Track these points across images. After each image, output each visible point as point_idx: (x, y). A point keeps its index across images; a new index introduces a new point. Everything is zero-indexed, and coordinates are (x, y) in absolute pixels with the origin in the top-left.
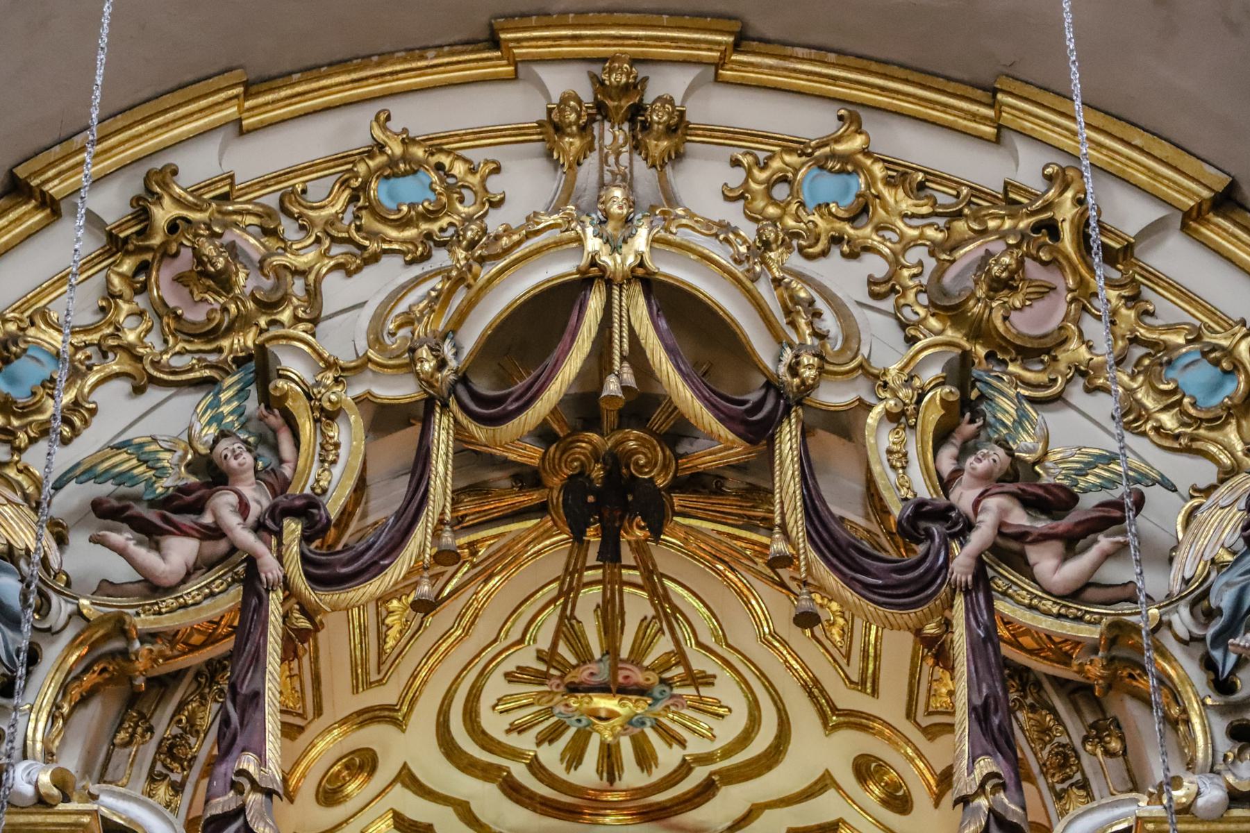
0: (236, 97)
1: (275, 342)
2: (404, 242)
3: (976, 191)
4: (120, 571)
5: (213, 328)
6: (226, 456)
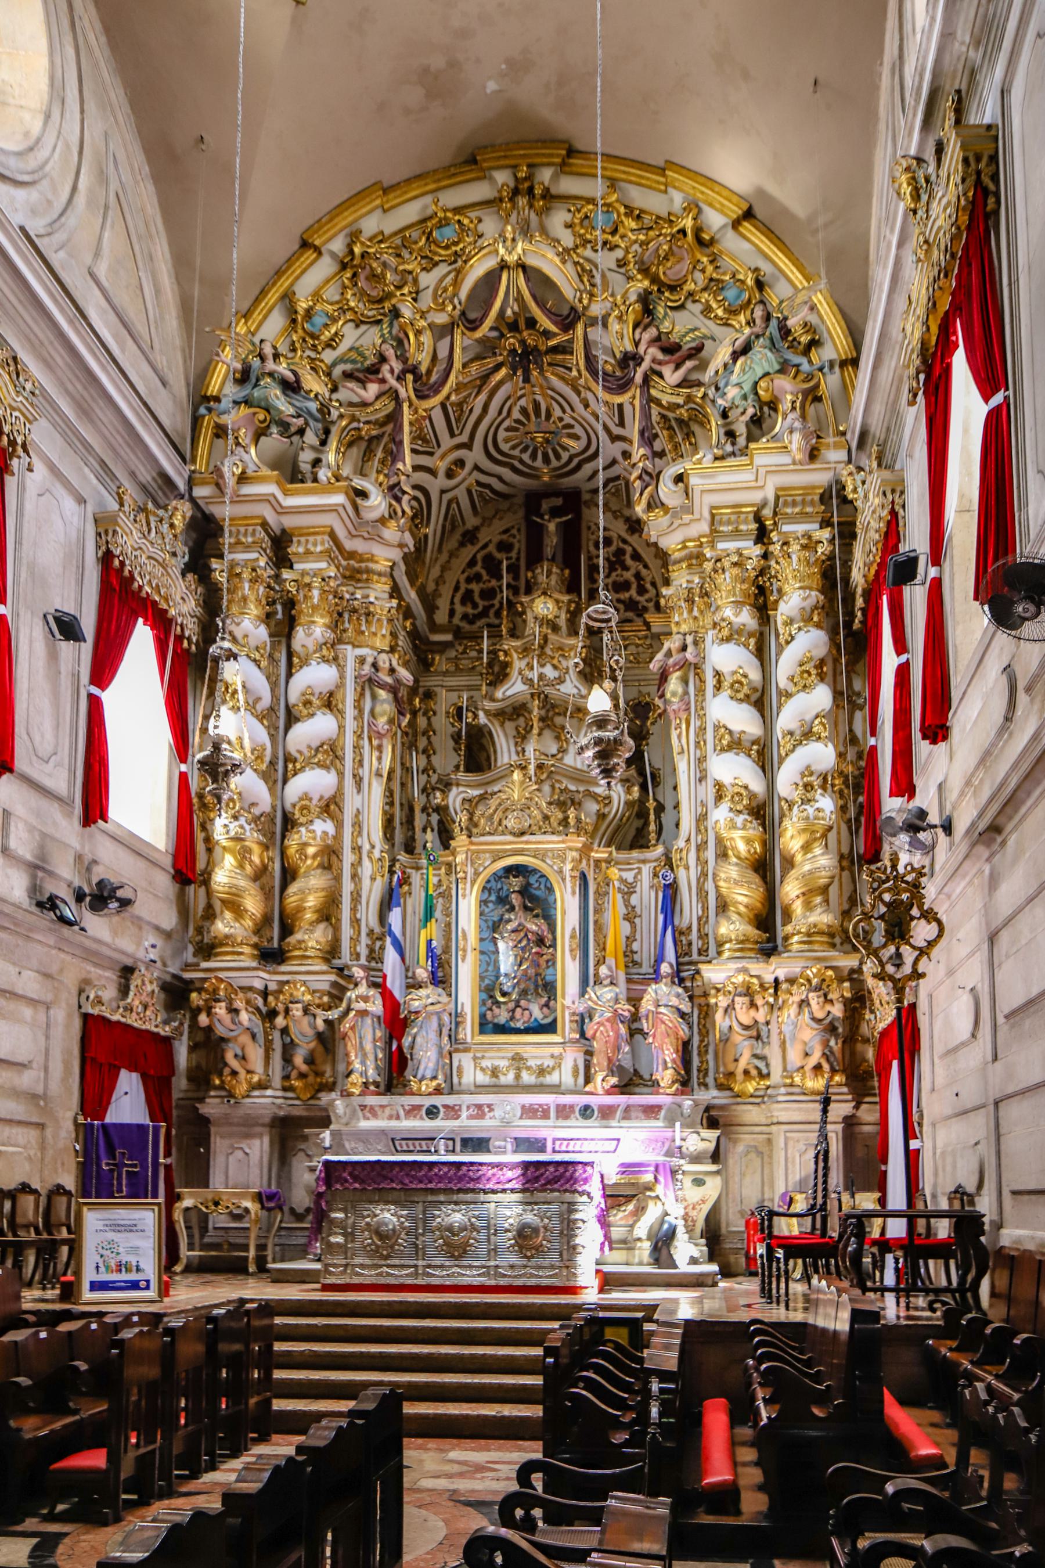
3: (658, 217)
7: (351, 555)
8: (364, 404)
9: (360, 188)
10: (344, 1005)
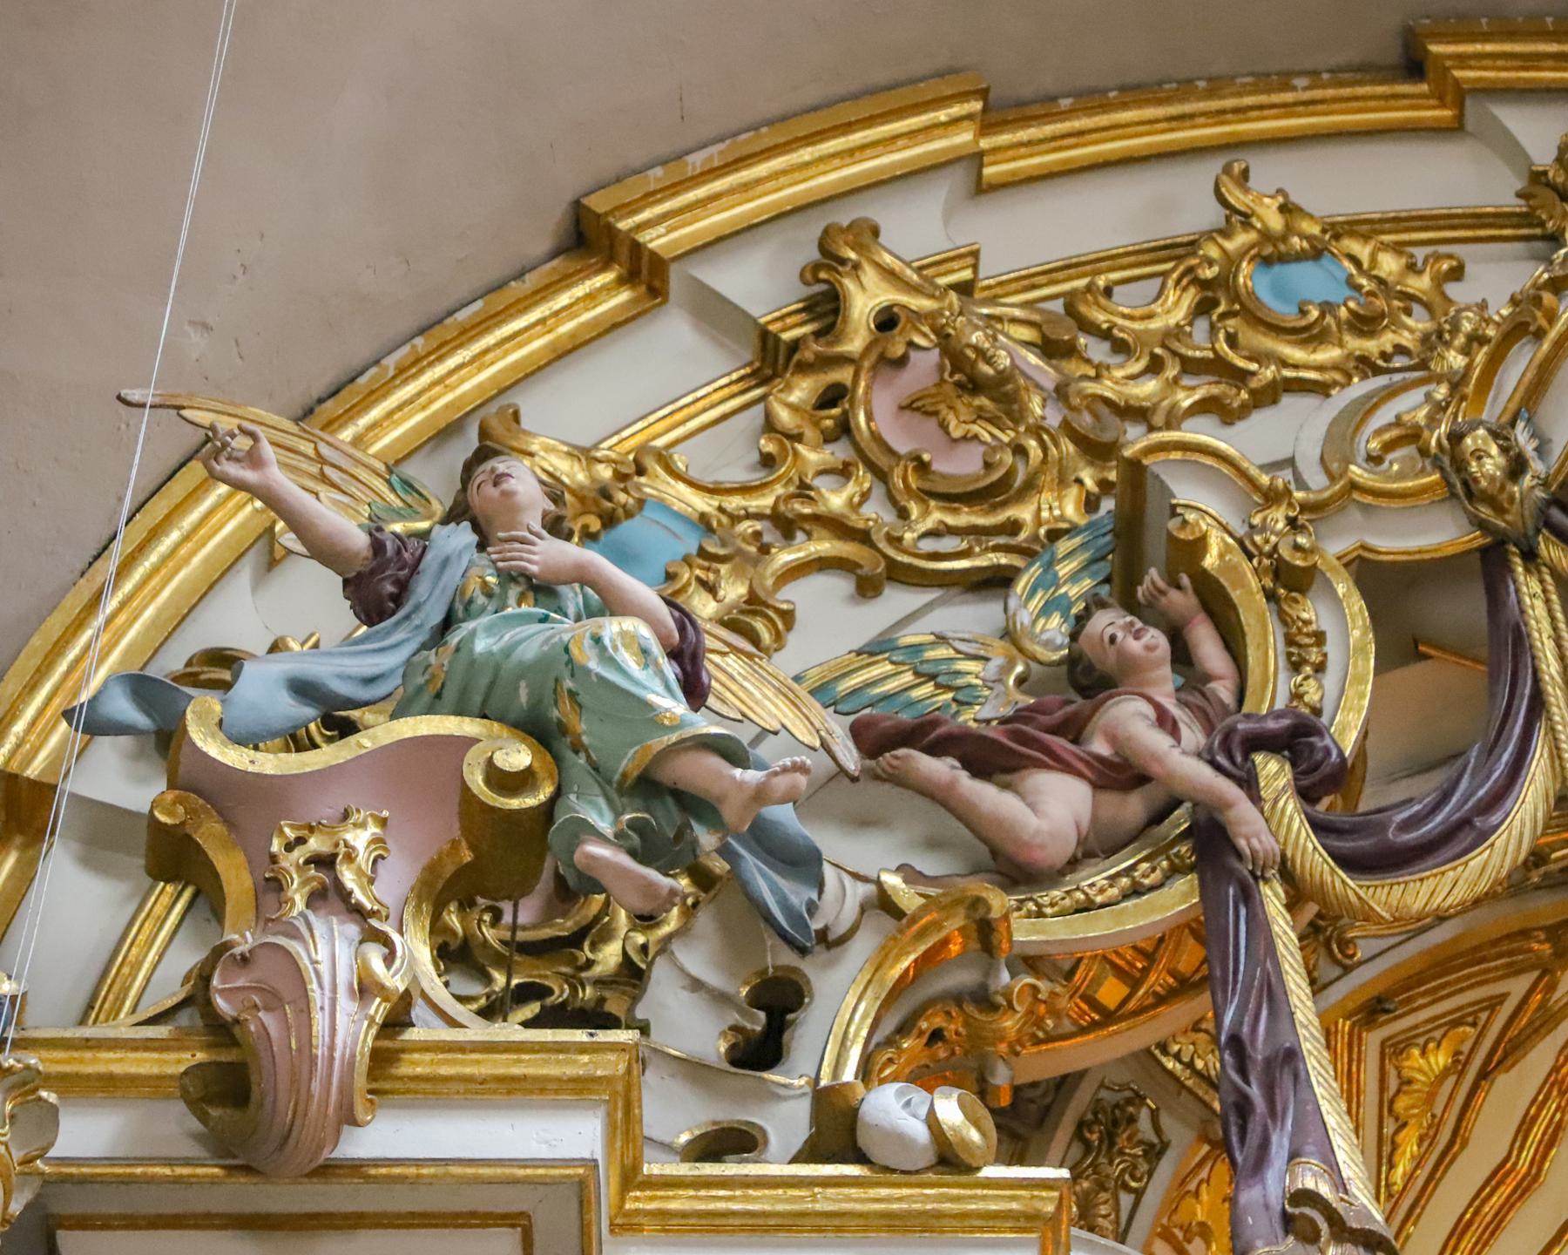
0: (969, 117)
1: (1162, 456)
2: (1320, 368)
5: (1000, 480)
6: (1113, 639)
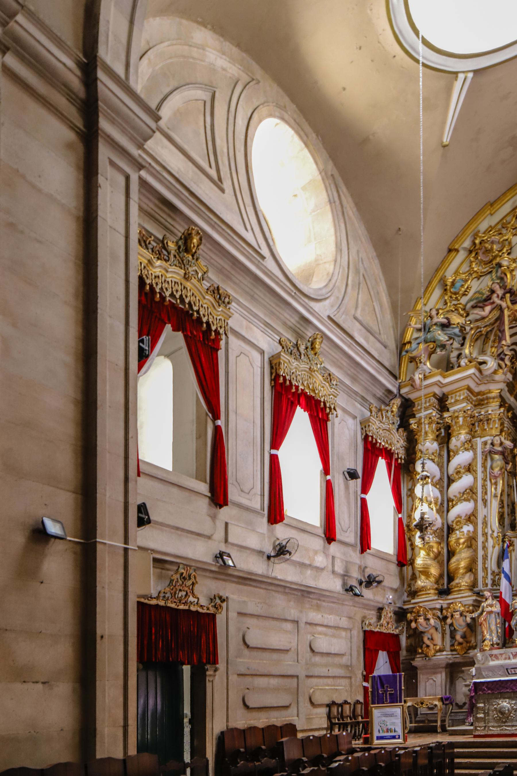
4: (478, 317)
7: (479, 394)
8: (483, 318)
9: (478, 210)
10: (480, 609)
